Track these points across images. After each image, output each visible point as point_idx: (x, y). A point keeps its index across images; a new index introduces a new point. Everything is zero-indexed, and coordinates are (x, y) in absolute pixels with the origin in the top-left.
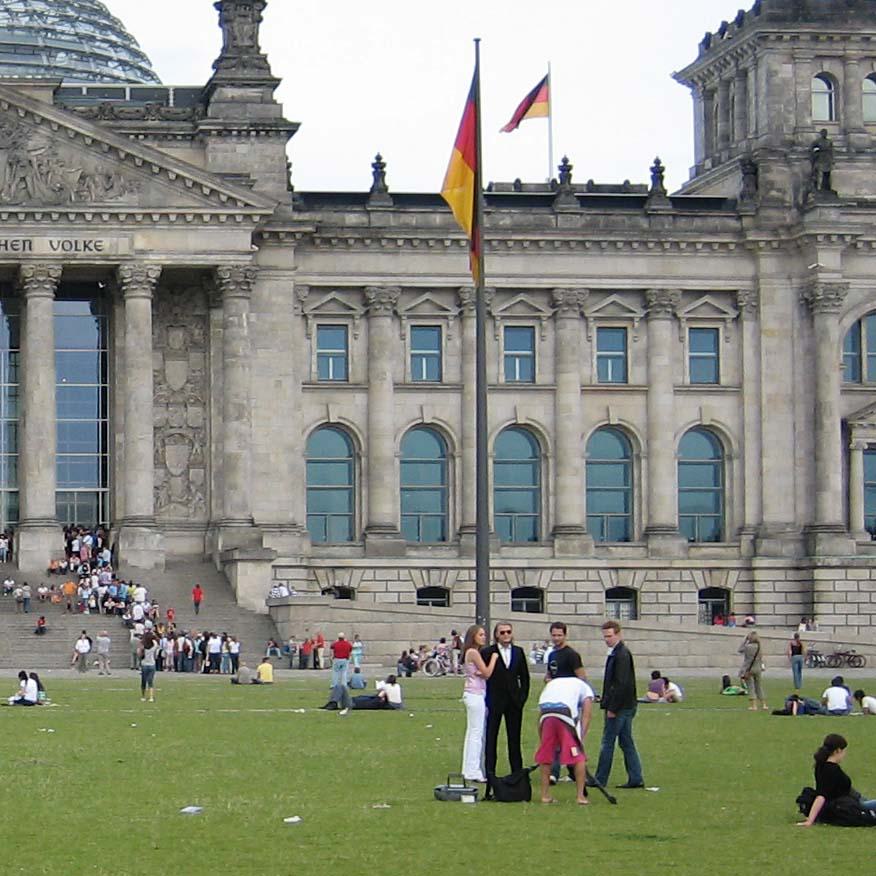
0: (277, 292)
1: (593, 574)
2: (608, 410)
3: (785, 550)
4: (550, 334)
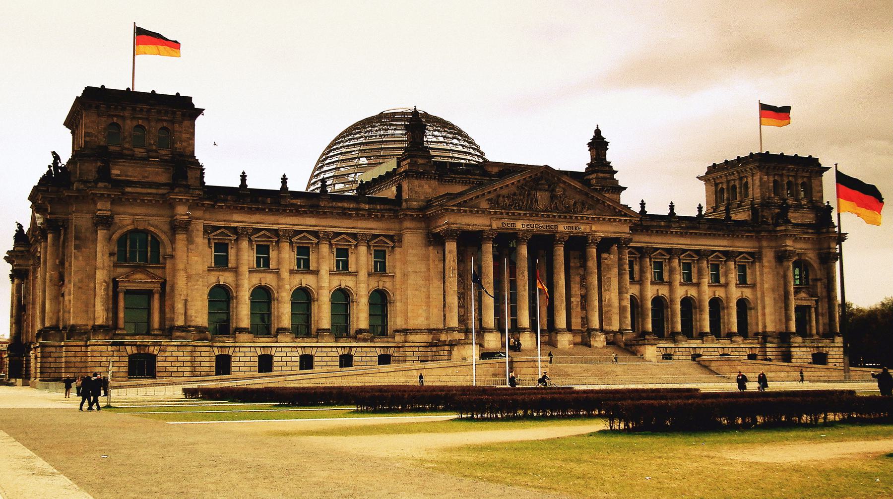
1: (716, 350)
2: (714, 292)
4: (696, 265)
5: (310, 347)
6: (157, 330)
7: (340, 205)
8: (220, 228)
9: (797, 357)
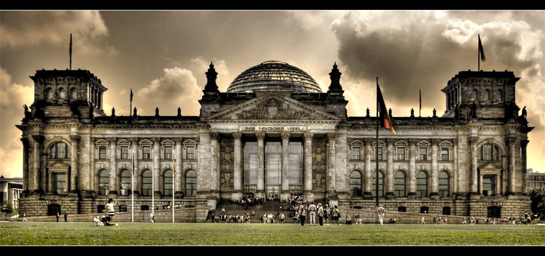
0: (343, 140)
1: (418, 204)
2: (422, 166)
3: (463, 198)
4: (408, 149)
5: (146, 201)
6: (66, 192)
7: (165, 122)
8: (100, 138)
9: (474, 209)
